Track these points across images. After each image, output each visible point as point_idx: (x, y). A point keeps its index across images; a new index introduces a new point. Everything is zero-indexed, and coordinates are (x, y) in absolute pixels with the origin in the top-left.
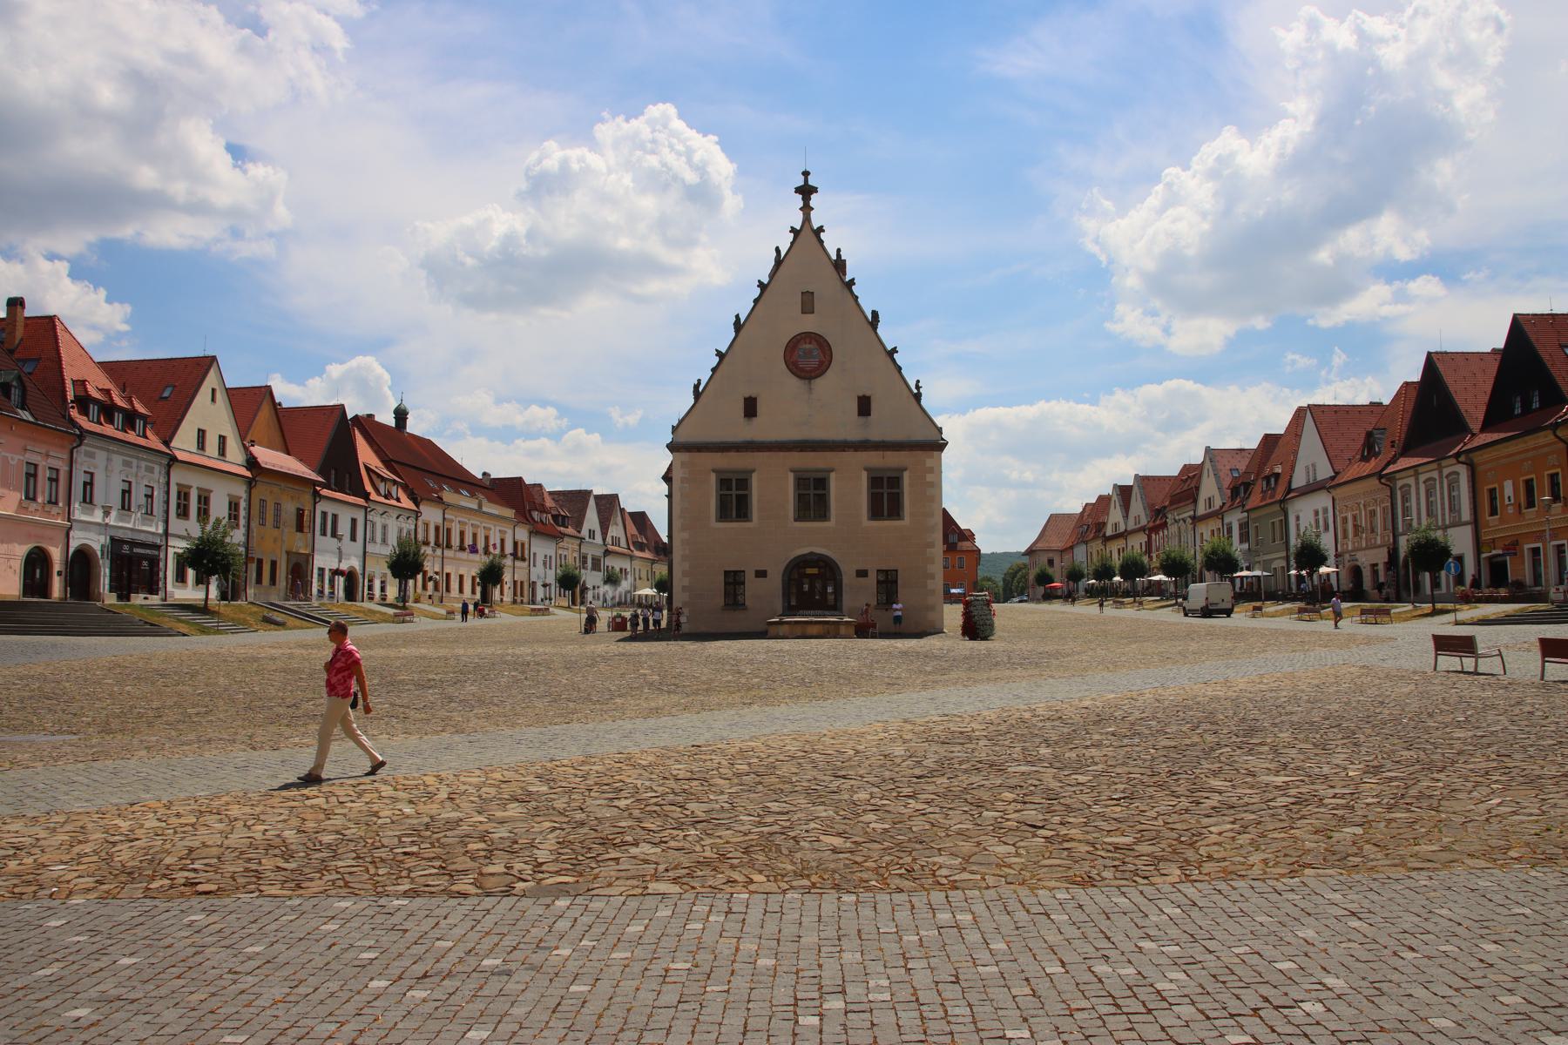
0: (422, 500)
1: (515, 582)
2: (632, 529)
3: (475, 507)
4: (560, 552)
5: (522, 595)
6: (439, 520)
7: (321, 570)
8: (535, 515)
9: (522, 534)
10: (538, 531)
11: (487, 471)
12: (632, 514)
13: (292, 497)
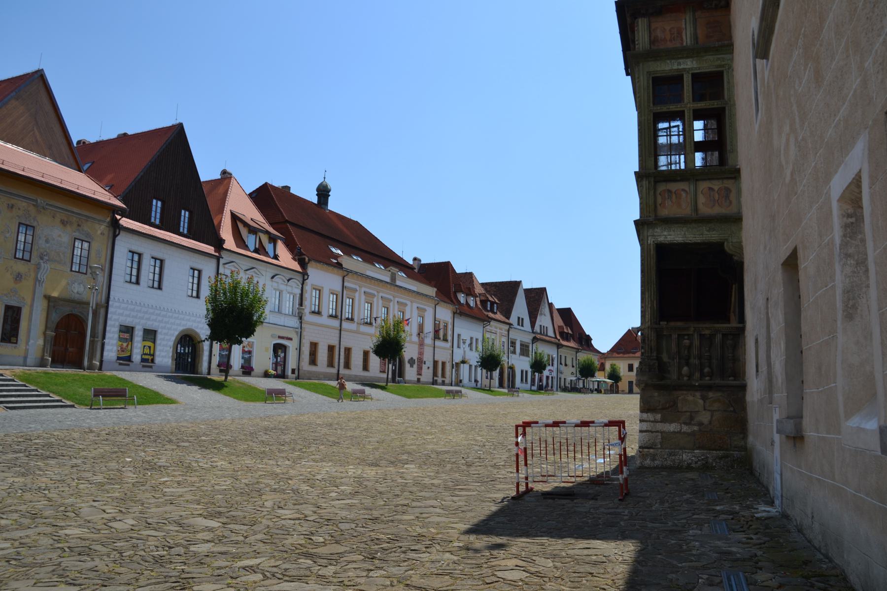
0: (309, 260)
1: (435, 363)
2: (559, 321)
3: (388, 279)
4: (487, 335)
5: (443, 375)
6: (338, 288)
7: (127, 331)
8: (462, 298)
9: (445, 313)
10: (463, 312)
11: (418, 257)
12: (559, 310)
13: (63, 223)
